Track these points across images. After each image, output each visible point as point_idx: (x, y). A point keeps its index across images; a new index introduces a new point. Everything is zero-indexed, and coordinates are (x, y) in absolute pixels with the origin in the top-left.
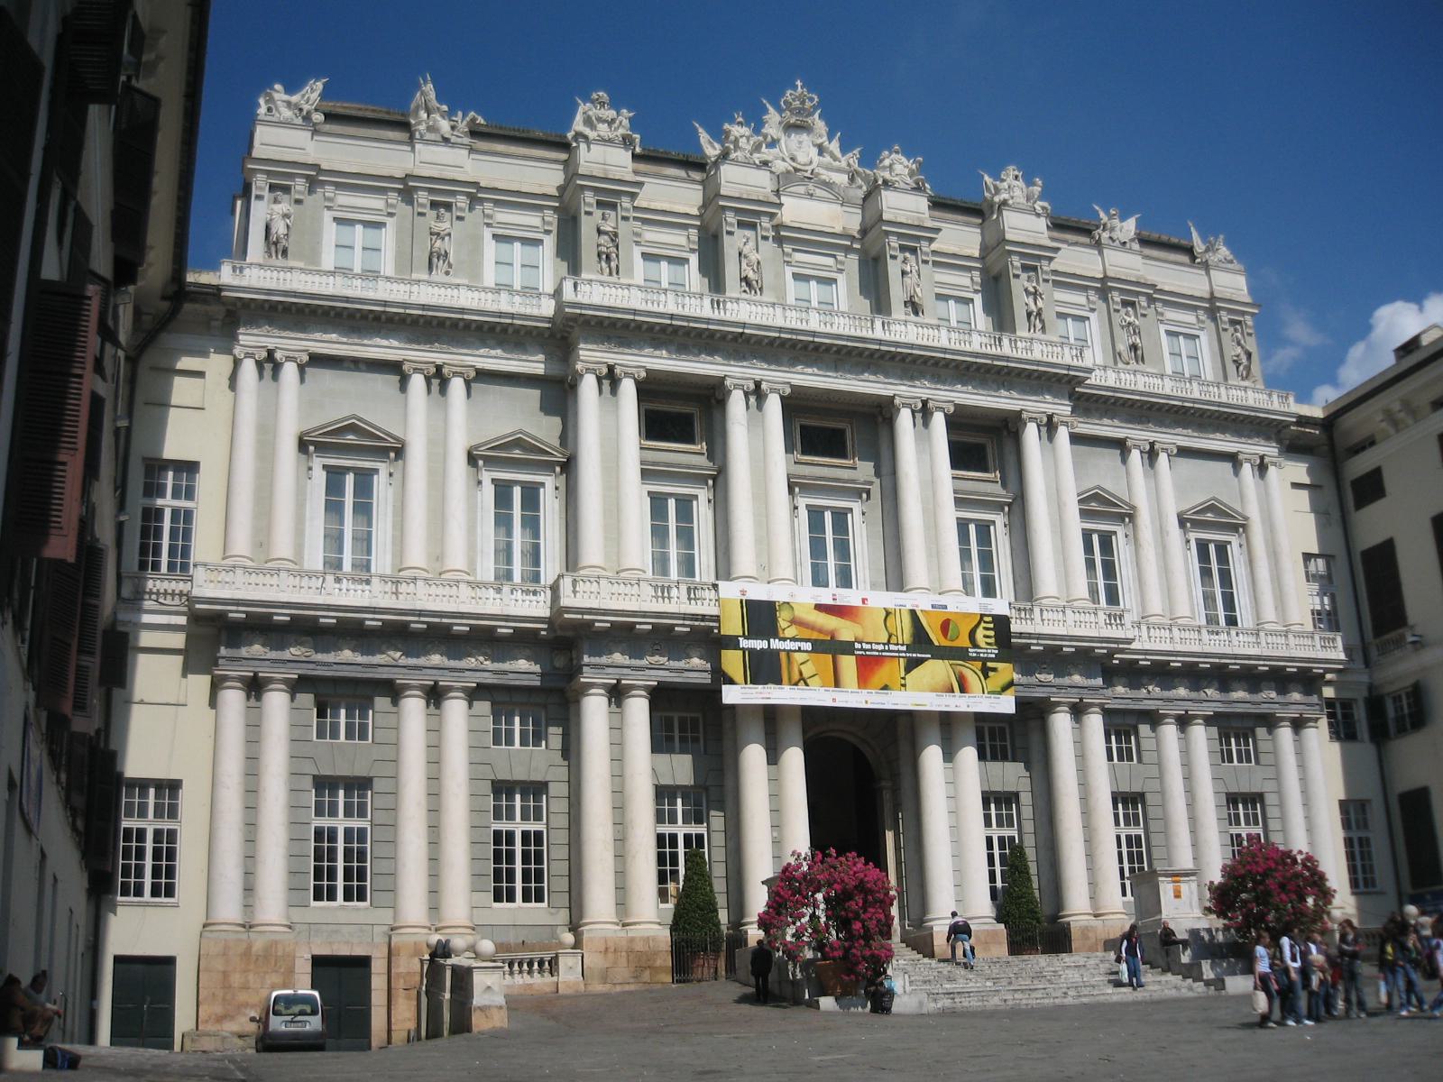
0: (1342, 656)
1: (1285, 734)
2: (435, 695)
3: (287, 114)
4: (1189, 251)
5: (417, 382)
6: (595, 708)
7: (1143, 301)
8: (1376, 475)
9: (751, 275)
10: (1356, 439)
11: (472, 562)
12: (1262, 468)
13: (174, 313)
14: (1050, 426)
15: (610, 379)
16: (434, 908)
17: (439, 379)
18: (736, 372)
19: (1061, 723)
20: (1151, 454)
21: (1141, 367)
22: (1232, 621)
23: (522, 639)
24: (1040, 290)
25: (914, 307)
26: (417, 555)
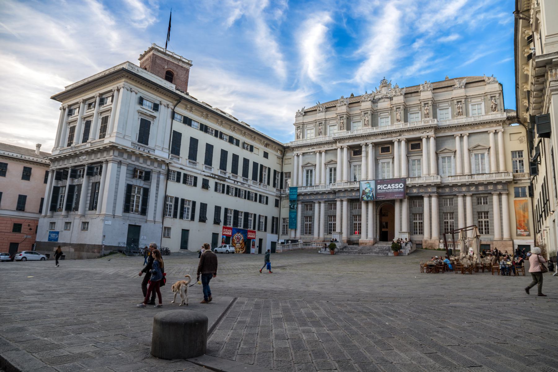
0: (512, 177)
1: (495, 198)
2: (320, 203)
3: (299, 114)
4: (484, 81)
5: (318, 154)
6: (338, 204)
7: (463, 100)
11: (325, 182)
12: (496, 133)
14: (428, 138)
16: (319, 235)
19: (426, 200)
21: (462, 117)
23: (329, 193)
26: (317, 182)
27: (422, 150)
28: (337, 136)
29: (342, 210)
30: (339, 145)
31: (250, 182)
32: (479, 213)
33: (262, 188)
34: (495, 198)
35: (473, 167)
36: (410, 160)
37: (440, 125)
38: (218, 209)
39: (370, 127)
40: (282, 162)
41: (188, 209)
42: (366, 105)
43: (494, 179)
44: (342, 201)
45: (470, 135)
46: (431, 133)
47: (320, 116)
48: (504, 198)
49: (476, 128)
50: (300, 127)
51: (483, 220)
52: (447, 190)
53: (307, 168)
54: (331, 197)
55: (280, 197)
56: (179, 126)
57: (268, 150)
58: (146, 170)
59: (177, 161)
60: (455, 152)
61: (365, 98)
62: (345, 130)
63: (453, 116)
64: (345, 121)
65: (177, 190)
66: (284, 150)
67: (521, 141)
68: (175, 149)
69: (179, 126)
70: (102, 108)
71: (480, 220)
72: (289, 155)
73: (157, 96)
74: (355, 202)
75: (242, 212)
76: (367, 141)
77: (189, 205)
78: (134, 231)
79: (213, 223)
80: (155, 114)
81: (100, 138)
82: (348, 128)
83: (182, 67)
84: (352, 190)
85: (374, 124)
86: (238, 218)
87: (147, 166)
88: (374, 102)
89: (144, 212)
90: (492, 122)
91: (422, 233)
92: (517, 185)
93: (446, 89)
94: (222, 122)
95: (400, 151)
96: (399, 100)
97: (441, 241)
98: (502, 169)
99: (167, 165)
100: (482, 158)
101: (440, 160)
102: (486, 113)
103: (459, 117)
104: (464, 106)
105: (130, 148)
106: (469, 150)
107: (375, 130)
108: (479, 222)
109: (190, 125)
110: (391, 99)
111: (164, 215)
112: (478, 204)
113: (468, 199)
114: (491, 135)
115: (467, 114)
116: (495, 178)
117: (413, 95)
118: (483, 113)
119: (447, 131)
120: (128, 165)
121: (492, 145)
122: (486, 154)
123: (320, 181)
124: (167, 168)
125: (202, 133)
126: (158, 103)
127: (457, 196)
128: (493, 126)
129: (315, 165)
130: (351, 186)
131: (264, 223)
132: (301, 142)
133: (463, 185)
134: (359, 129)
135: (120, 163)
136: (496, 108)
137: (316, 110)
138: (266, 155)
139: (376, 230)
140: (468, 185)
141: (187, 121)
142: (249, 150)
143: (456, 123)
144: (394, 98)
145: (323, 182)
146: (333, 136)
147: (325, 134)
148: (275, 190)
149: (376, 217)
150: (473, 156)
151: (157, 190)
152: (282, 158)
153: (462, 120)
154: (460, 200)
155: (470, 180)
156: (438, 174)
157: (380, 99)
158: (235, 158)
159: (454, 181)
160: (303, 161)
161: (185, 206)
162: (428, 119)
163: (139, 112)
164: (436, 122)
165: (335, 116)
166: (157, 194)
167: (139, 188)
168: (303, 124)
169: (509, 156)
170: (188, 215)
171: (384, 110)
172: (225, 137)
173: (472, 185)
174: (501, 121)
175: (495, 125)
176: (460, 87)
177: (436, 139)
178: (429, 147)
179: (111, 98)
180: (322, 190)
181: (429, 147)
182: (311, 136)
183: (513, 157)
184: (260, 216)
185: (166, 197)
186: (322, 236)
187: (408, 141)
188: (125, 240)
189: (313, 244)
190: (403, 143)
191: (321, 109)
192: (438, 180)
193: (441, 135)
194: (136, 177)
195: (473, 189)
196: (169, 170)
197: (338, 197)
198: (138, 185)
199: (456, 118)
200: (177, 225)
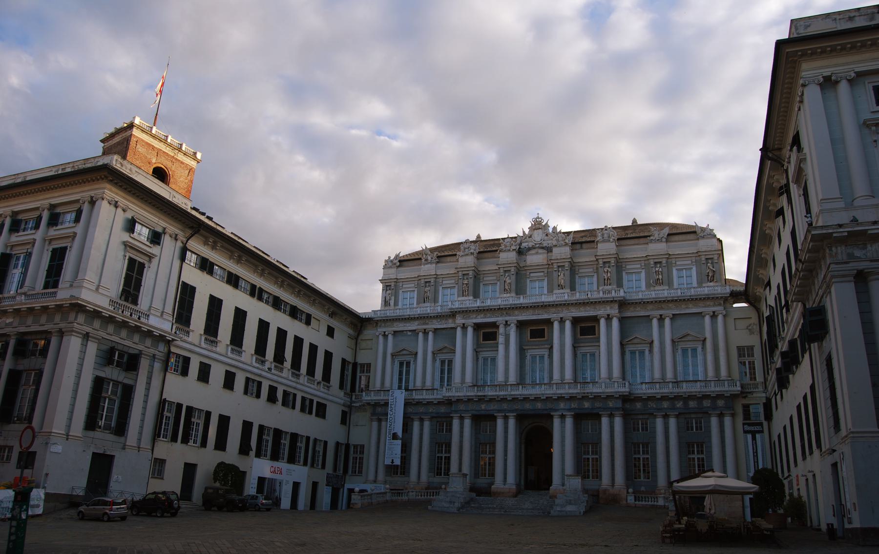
0: (739, 389)
1: (714, 421)
2: (422, 420)
3: (390, 264)
4: (695, 232)
5: (421, 334)
6: (456, 423)
9: (507, 287)
11: (433, 383)
12: (714, 316)
14: (609, 318)
15: (464, 327)
17: (426, 333)
18: (499, 319)
20: (661, 319)
23: (440, 403)
25: (561, 287)
27: (599, 338)
28: (457, 305)
29: (462, 432)
30: (459, 320)
31: (304, 379)
32: (690, 445)
33: (322, 390)
34: (714, 421)
35: (680, 368)
36: (578, 352)
37: (628, 298)
38: (247, 426)
39: (513, 294)
41: (198, 424)
42: (508, 257)
43: (713, 389)
44: (462, 418)
45: (674, 317)
46: (614, 311)
47: (428, 269)
48: (727, 421)
49: (683, 306)
50: (390, 287)
51: (696, 456)
52: (639, 405)
53: (402, 358)
54: (443, 409)
55: (350, 407)
56: (192, 275)
57: (334, 323)
58: (131, 351)
59: (186, 338)
61: (506, 246)
62: (471, 298)
63: (648, 286)
64: (471, 281)
65: (182, 390)
66: (359, 323)
67: (751, 332)
68: (183, 315)
69: (192, 275)
70: (53, 232)
71: (691, 456)
72: (369, 333)
73: (160, 218)
74: (483, 420)
75: (286, 433)
76: (507, 318)
77: (199, 418)
78: (101, 465)
79: (237, 451)
80: (155, 250)
81: (46, 286)
82: (476, 295)
83: (182, 163)
84: (481, 399)
85: (520, 290)
86: (280, 443)
87: (133, 344)
88: (521, 252)
89: (121, 429)
90: (709, 298)
91: (598, 475)
92: (745, 402)
93: (636, 241)
94: (263, 270)
95: (562, 337)
96: (562, 252)
97: (631, 490)
98: (723, 372)
99: (169, 343)
100: (694, 355)
101: (628, 356)
102: (700, 283)
103: (657, 288)
104: (665, 270)
105: (108, 310)
106: (673, 341)
107: (522, 300)
108: (690, 459)
109: (211, 272)
110: (549, 250)
111: (156, 435)
112: (688, 430)
113: (672, 422)
114: (707, 319)
115: (670, 284)
116: (713, 389)
117: (584, 246)
118: (695, 284)
119: (638, 309)
120: (100, 341)
121: (708, 334)
122: (699, 349)
123: (424, 382)
124: (166, 349)
125: (229, 288)
126: (159, 230)
127: (655, 417)
128: (709, 306)
129: (416, 354)
130: (480, 394)
131: (321, 453)
132: (390, 313)
133: (664, 398)
134: (495, 296)
135: (86, 337)
136: (713, 276)
137: (420, 259)
138: (330, 332)
139: (520, 470)
140: (671, 398)
141: (206, 266)
142: (304, 321)
143: (654, 296)
144: (554, 249)
145: (428, 384)
146: (450, 306)
147: (435, 300)
148: (342, 394)
149: (520, 448)
150: (680, 351)
151: (148, 389)
152: (356, 339)
153: (664, 292)
154: (659, 422)
155: (676, 390)
156: (624, 379)
157: (529, 249)
158: (282, 334)
159: (650, 391)
160: (395, 345)
161: (193, 420)
162: (609, 287)
163: (126, 244)
164: (622, 294)
165: (453, 271)
166: (147, 396)
167: (116, 383)
168: (397, 281)
169: (734, 353)
170: (196, 436)
171: (538, 267)
172: (265, 296)
173: (677, 398)
174: (721, 297)
175: (712, 303)
176: (659, 240)
177: (622, 320)
178: (609, 335)
179: (74, 215)
180: (427, 397)
181: (609, 335)
182: (409, 303)
183: (740, 356)
184: (316, 440)
185: (162, 403)
186: (424, 478)
187: (575, 321)
188: (84, 483)
189: (411, 494)
190: (568, 325)
191: (429, 258)
192: (625, 390)
193: (628, 314)
194: (112, 364)
195: (679, 404)
196: (169, 352)
197: (456, 412)
198: (114, 378)
199: (652, 288)
200: (176, 455)
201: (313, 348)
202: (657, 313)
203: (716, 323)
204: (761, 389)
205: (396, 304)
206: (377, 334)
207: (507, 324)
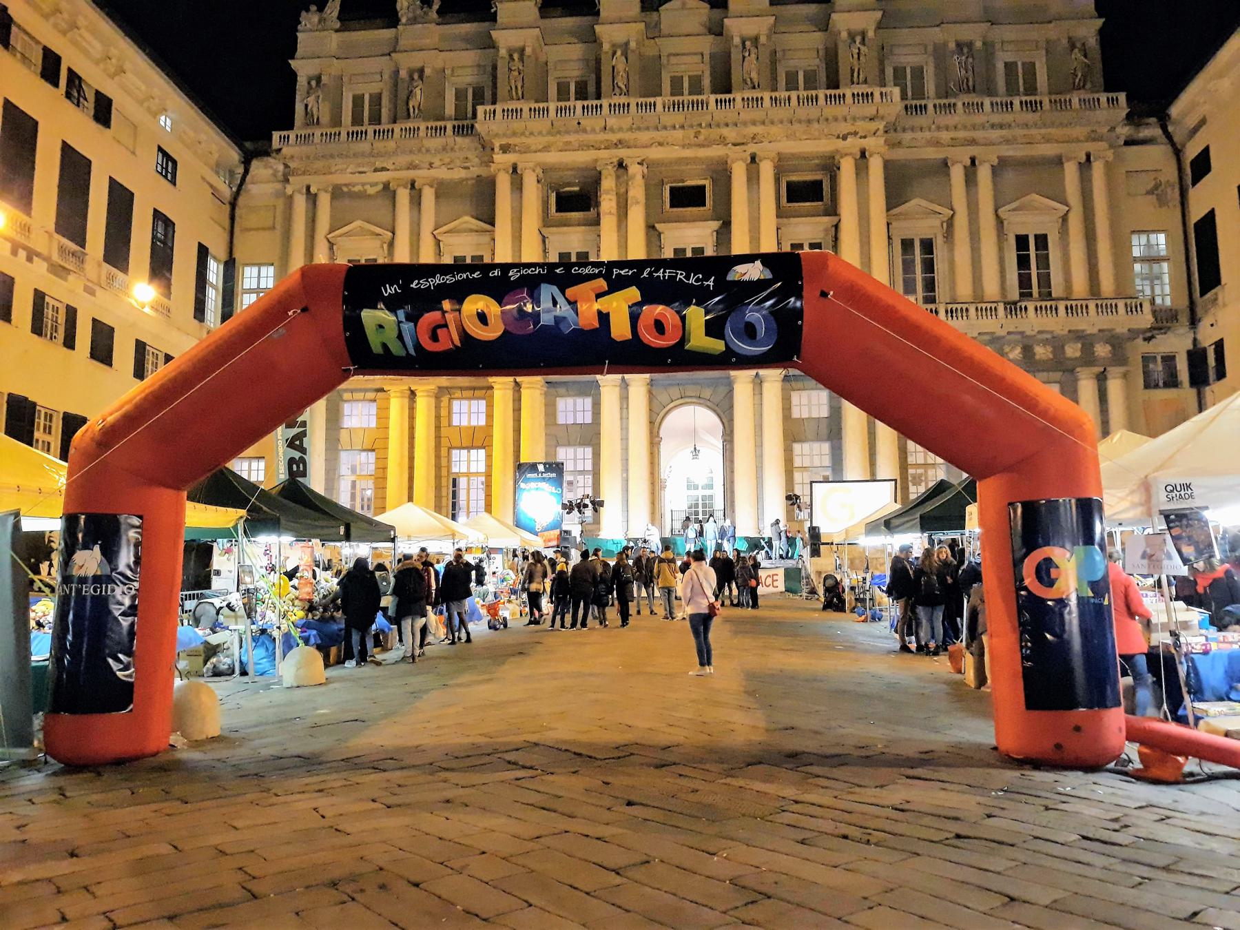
5: (403, 196)
8: (1206, 151)
10: (1191, 122)
13: (246, 171)
22: (1047, 295)
24: (863, 48)
40: (232, 218)
46: (875, 144)
48: (1115, 387)
60: (950, 222)
67: (1162, 202)
76: (622, 153)
98: (1107, 284)
114: (1071, 171)
128: (1078, 140)
138: (168, 166)
190: (767, 171)
193: (900, 154)
201: (121, 200)
202: (964, 154)
203: (1090, 181)
204: (1184, 319)
205: (336, 121)
206: (289, 190)
207: (621, 165)
